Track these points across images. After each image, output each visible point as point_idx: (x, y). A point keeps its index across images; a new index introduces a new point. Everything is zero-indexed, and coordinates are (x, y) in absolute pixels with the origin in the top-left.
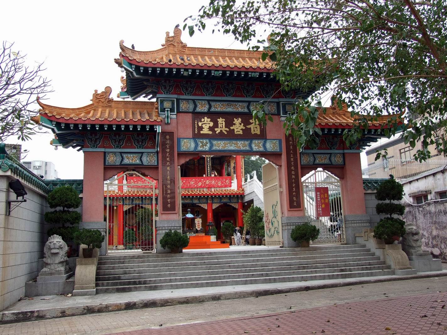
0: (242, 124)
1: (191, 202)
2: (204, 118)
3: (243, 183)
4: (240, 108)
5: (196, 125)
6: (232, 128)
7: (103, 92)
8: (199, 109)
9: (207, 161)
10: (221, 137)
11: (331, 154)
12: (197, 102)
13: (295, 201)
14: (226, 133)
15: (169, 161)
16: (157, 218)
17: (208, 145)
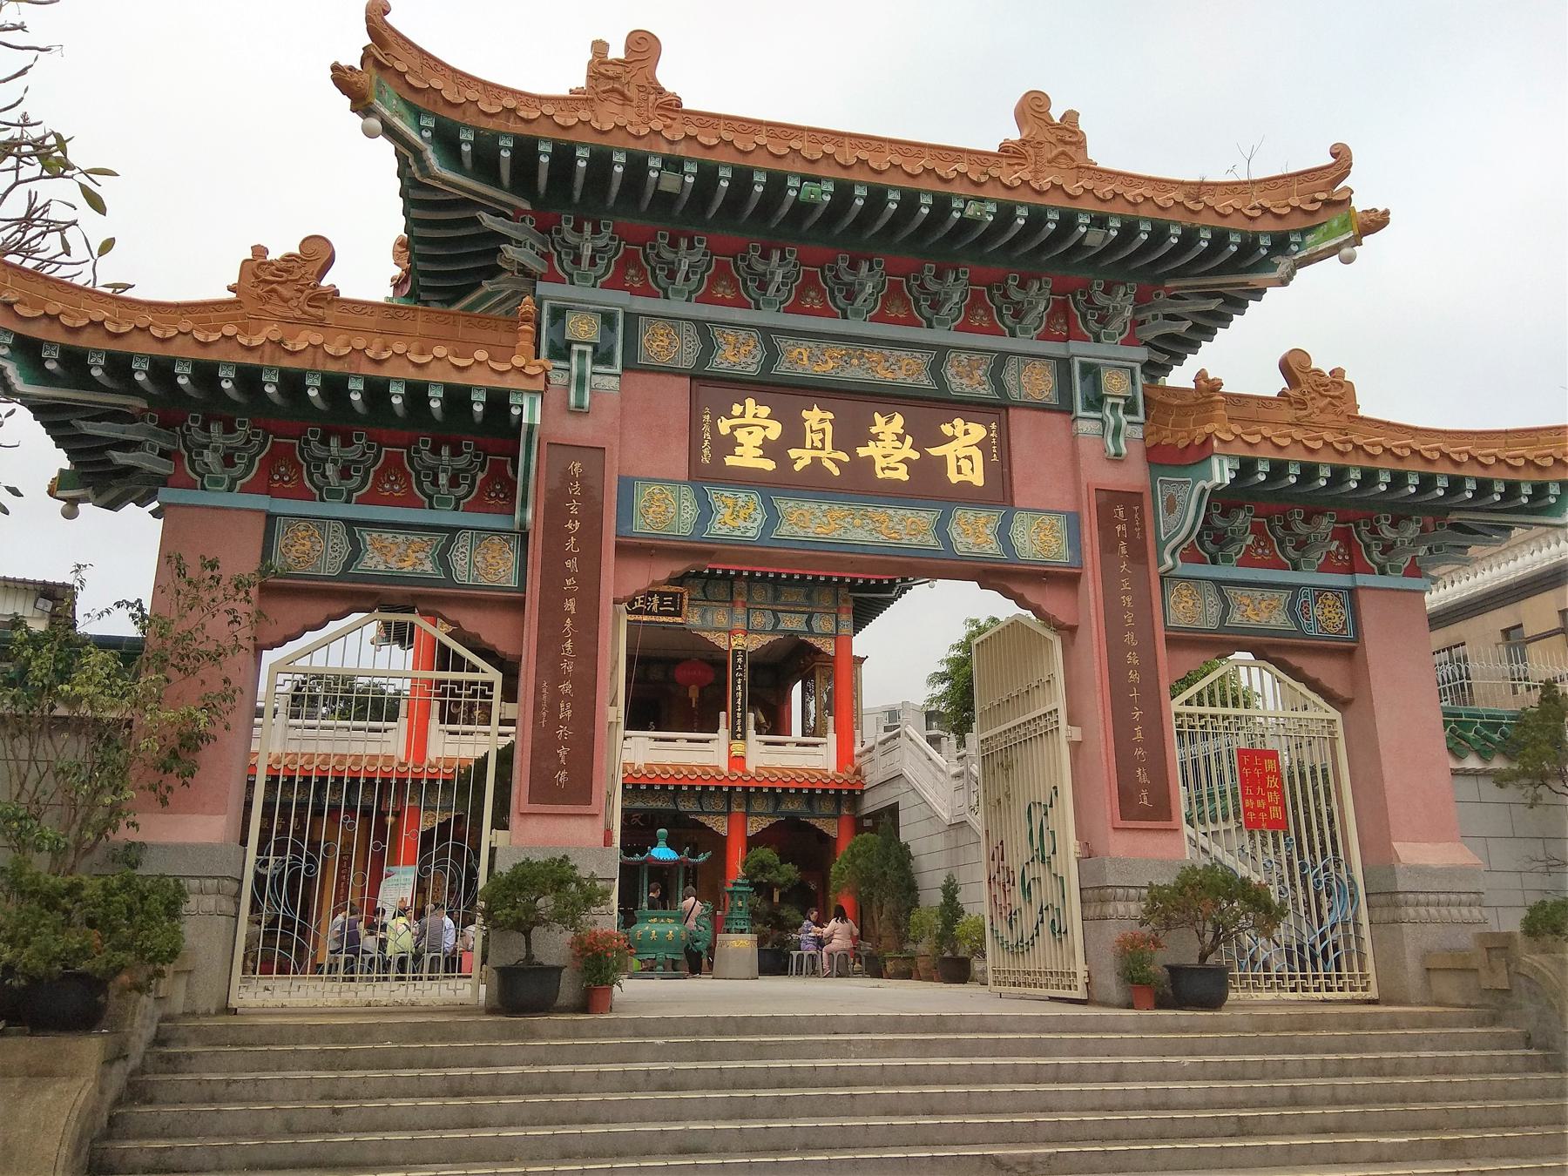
0: (909, 440)
1: (671, 806)
2: (743, 404)
4: (905, 371)
5: (706, 427)
6: (862, 452)
7: (289, 258)
9: (735, 664)
10: (814, 485)
11: (1295, 588)
13: (1145, 786)
14: (836, 472)
15: (574, 575)
17: (760, 517)
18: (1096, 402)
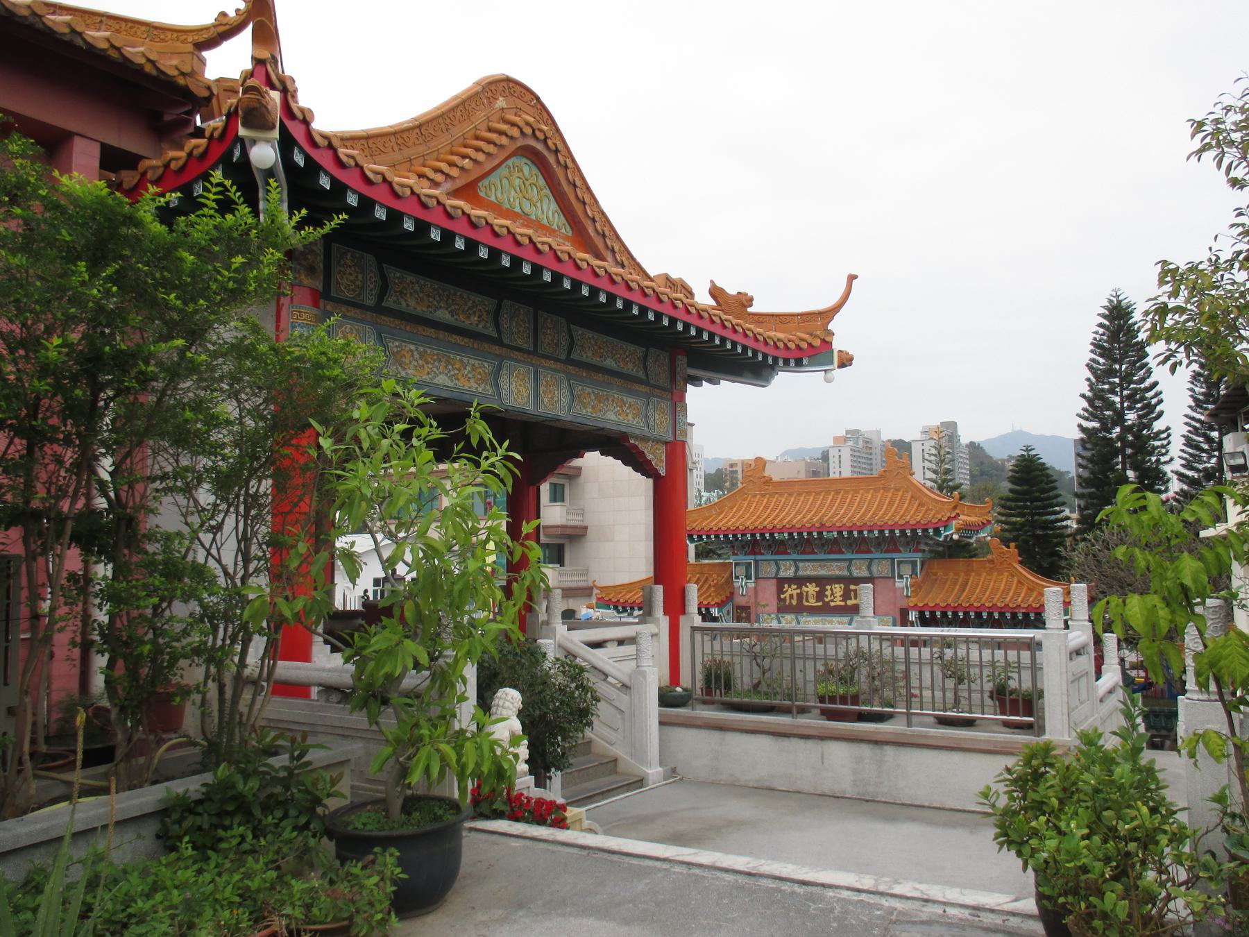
4: (836, 569)
8: (782, 574)
12: (779, 562)
18: (901, 577)
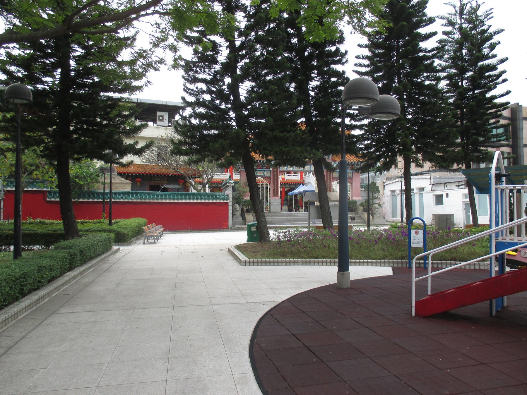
3: (304, 176)
16: (270, 198)
